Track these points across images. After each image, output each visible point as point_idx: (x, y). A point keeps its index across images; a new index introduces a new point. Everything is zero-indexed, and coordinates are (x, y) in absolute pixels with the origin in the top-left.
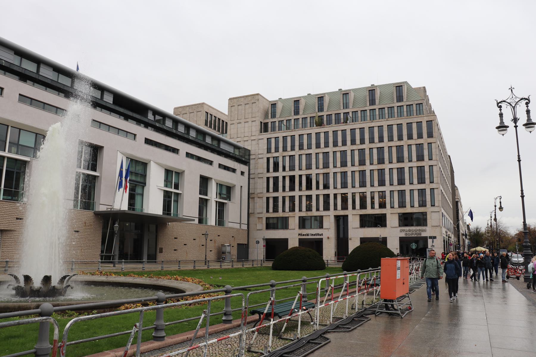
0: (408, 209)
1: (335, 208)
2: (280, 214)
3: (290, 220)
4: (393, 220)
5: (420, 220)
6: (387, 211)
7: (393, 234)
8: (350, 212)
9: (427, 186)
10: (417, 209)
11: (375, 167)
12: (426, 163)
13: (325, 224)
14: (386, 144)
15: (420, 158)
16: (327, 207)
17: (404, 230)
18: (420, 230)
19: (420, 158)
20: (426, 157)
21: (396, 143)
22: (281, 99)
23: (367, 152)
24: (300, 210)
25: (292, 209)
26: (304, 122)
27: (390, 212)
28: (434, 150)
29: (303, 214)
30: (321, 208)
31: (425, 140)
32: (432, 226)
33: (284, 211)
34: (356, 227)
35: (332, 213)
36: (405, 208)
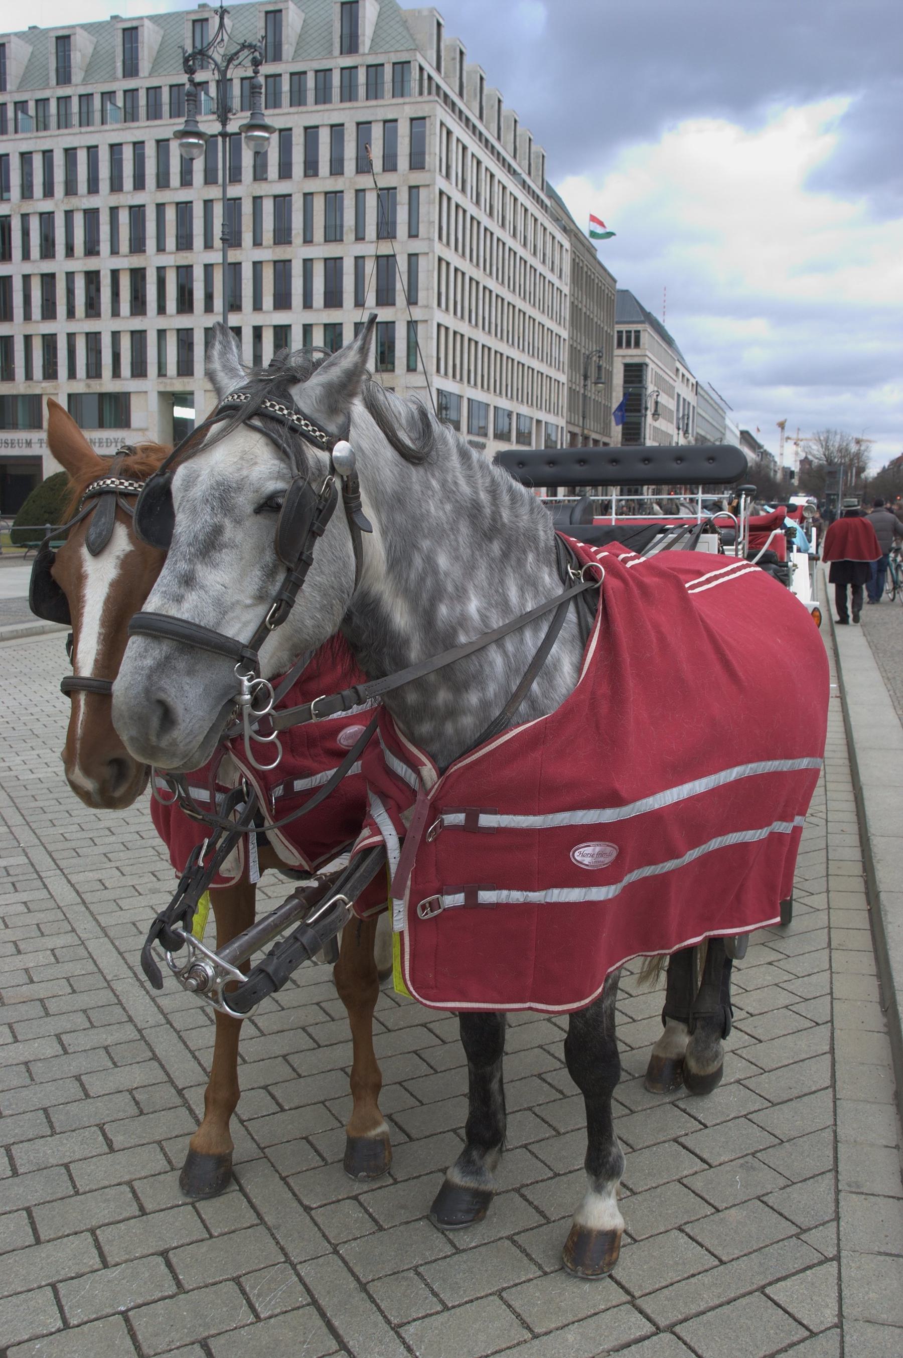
1: (161, 373)
11: (267, 254)
12: (401, 247)
13: (137, 417)
15: (386, 231)
16: (139, 370)
19: (386, 231)
20: (402, 229)
21: (324, 182)
22: (35, 27)
24: (72, 374)
26: (84, 109)
28: (423, 210)
31: (401, 178)
33: (29, 376)
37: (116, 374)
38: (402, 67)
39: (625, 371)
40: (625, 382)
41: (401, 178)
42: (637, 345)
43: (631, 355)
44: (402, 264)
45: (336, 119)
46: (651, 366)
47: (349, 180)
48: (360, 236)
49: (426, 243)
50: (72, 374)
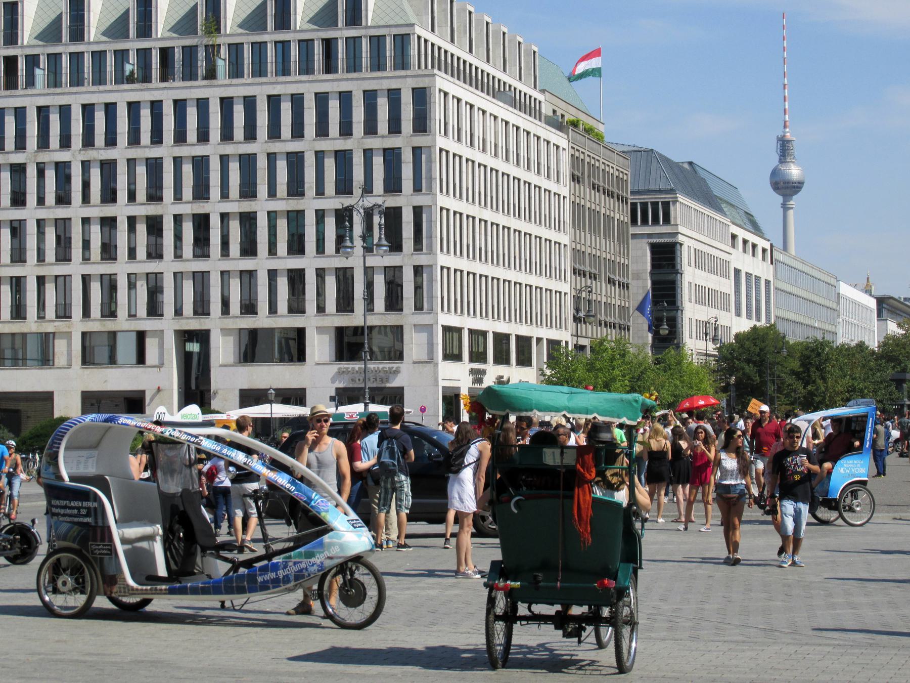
1: (178, 312)
2: (31, 324)
3: (60, 346)
6: (309, 321)
8: (214, 323)
10: (380, 317)
16: (154, 310)
17: (346, 372)
23: (262, 163)
24: (86, 313)
25: (64, 313)
29: (96, 324)
31: (405, 141)
32: (415, 363)
35: (168, 325)
38: (402, 41)
40: (654, 266)
41: (405, 141)
42: (667, 220)
44: (408, 217)
45: (344, 87)
50: (86, 313)
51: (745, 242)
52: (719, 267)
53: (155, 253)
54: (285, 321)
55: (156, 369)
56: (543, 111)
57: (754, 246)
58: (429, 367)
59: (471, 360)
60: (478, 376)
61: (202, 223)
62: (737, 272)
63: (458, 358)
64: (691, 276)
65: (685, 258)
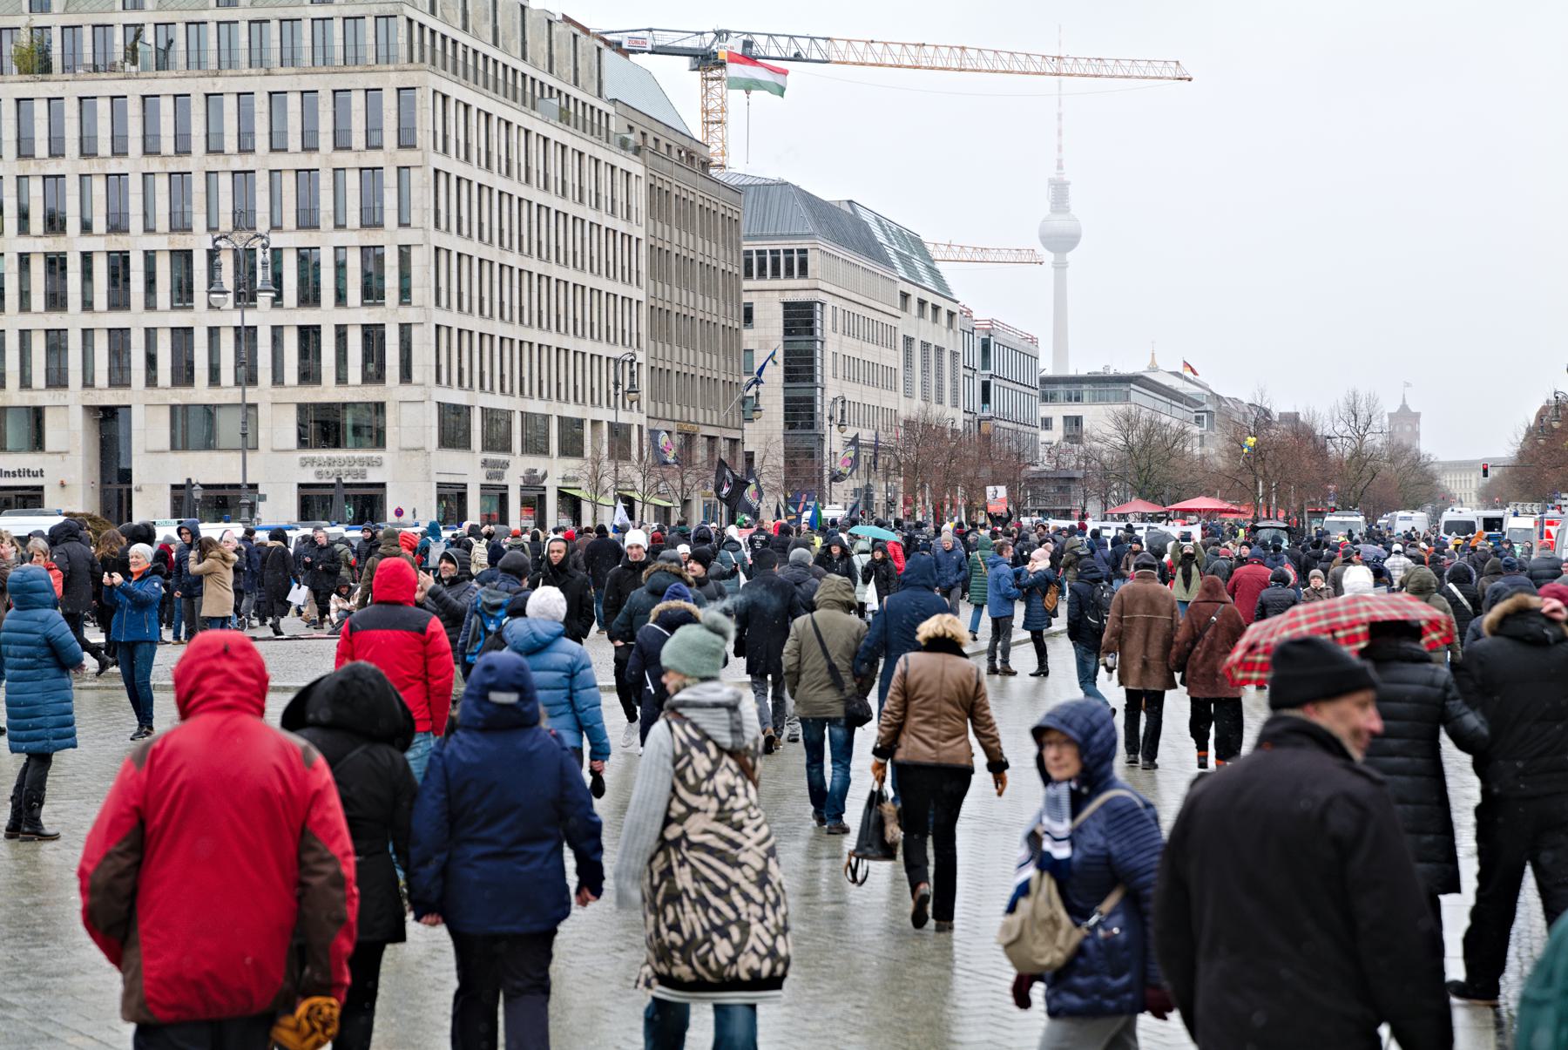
0: (327, 392)
4: (279, 425)
5: (368, 428)
7: (279, 471)
8: (135, 396)
9: (389, 315)
10: (356, 391)
14: (261, 161)
17: (313, 461)
18: (361, 461)
19: (372, 220)
20: (390, 218)
27: (269, 399)
30: (39, 378)
32: (401, 449)
34: (160, 447)
36: (316, 388)
37: (25, 383)
39: (786, 315)
40: (787, 332)
43: (796, 289)
46: (830, 301)
47: (325, 159)
48: (341, 222)
49: (420, 232)
51: (922, 303)
52: (884, 336)
53: (56, 301)
54: (228, 393)
55: (58, 457)
56: (612, 128)
57: (936, 308)
58: (418, 459)
59: (485, 448)
60: (496, 469)
61: (119, 266)
62: (908, 341)
63: (465, 444)
64: (833, 345)
65: (826, 324)
